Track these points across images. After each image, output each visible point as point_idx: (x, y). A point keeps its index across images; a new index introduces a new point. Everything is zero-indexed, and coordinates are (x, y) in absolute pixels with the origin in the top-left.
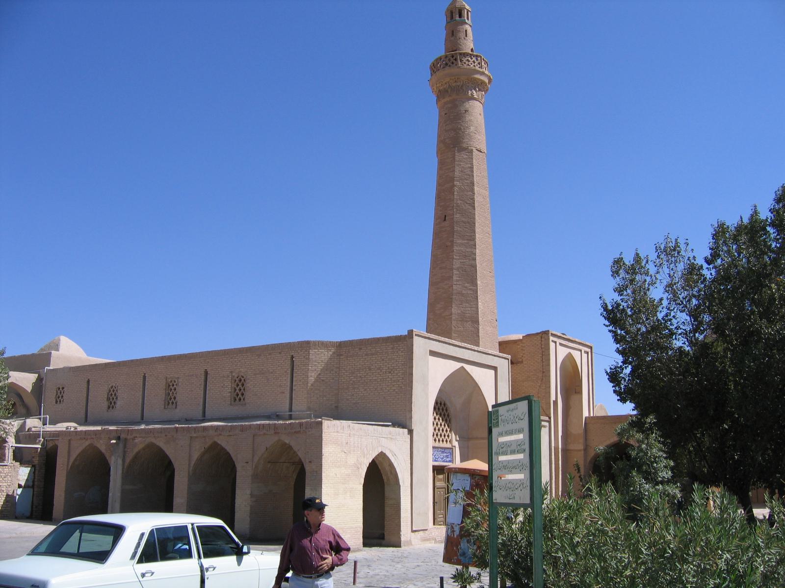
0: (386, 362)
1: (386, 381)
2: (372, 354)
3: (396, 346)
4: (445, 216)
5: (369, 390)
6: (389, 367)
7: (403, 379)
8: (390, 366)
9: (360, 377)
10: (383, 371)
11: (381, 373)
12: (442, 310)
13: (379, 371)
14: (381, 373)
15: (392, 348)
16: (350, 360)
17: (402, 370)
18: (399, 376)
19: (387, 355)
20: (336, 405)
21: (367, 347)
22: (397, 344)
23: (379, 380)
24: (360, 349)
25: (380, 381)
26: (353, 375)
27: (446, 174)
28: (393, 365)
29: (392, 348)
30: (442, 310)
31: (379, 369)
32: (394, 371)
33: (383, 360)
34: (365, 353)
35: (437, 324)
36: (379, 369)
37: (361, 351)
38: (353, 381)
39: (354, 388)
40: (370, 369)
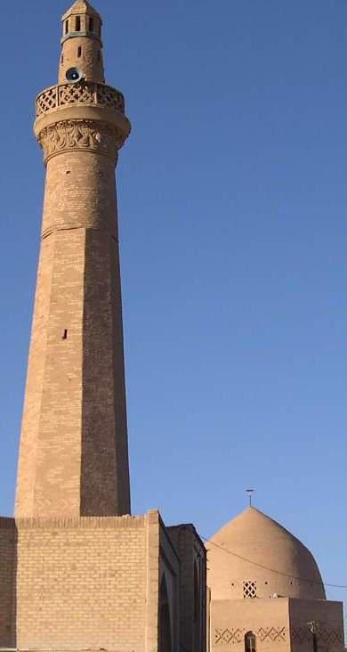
0: (105, 559)
1: (105, 588)
2: (78, 544)
3: (125, 533)
4: (66, 331)
5: (71, 601)
6: (110, 567)
7: (137, 587)
8: (113, 565)
9: (56, 580)
10: (99, 572)
11: (95, 576)
12: (60, 480)
13: (93, 572)
14: (95, 576)
15: (117, 537)
16: (33, 550)
17: (136, 573)
18: (130, 582)
19: (106, 547)
20: (8, 623)
21: (67, 532)
22: (126, 531)
23: (92, 587)
24: (55, 534)
25: (95, 588)
26: (42, 576)
27: (68, 267)
28: (118, 564)
29: (117, 537)
30: (60, 480)
31: (91, 569)
32: (120, 575)
33: (99, 555)
34: (65, 541)
35: (51, 501)
36: (91, 569)
37: (57, 537)
38: (42, 586)
39: (43, 598)
40: (74, 568)
